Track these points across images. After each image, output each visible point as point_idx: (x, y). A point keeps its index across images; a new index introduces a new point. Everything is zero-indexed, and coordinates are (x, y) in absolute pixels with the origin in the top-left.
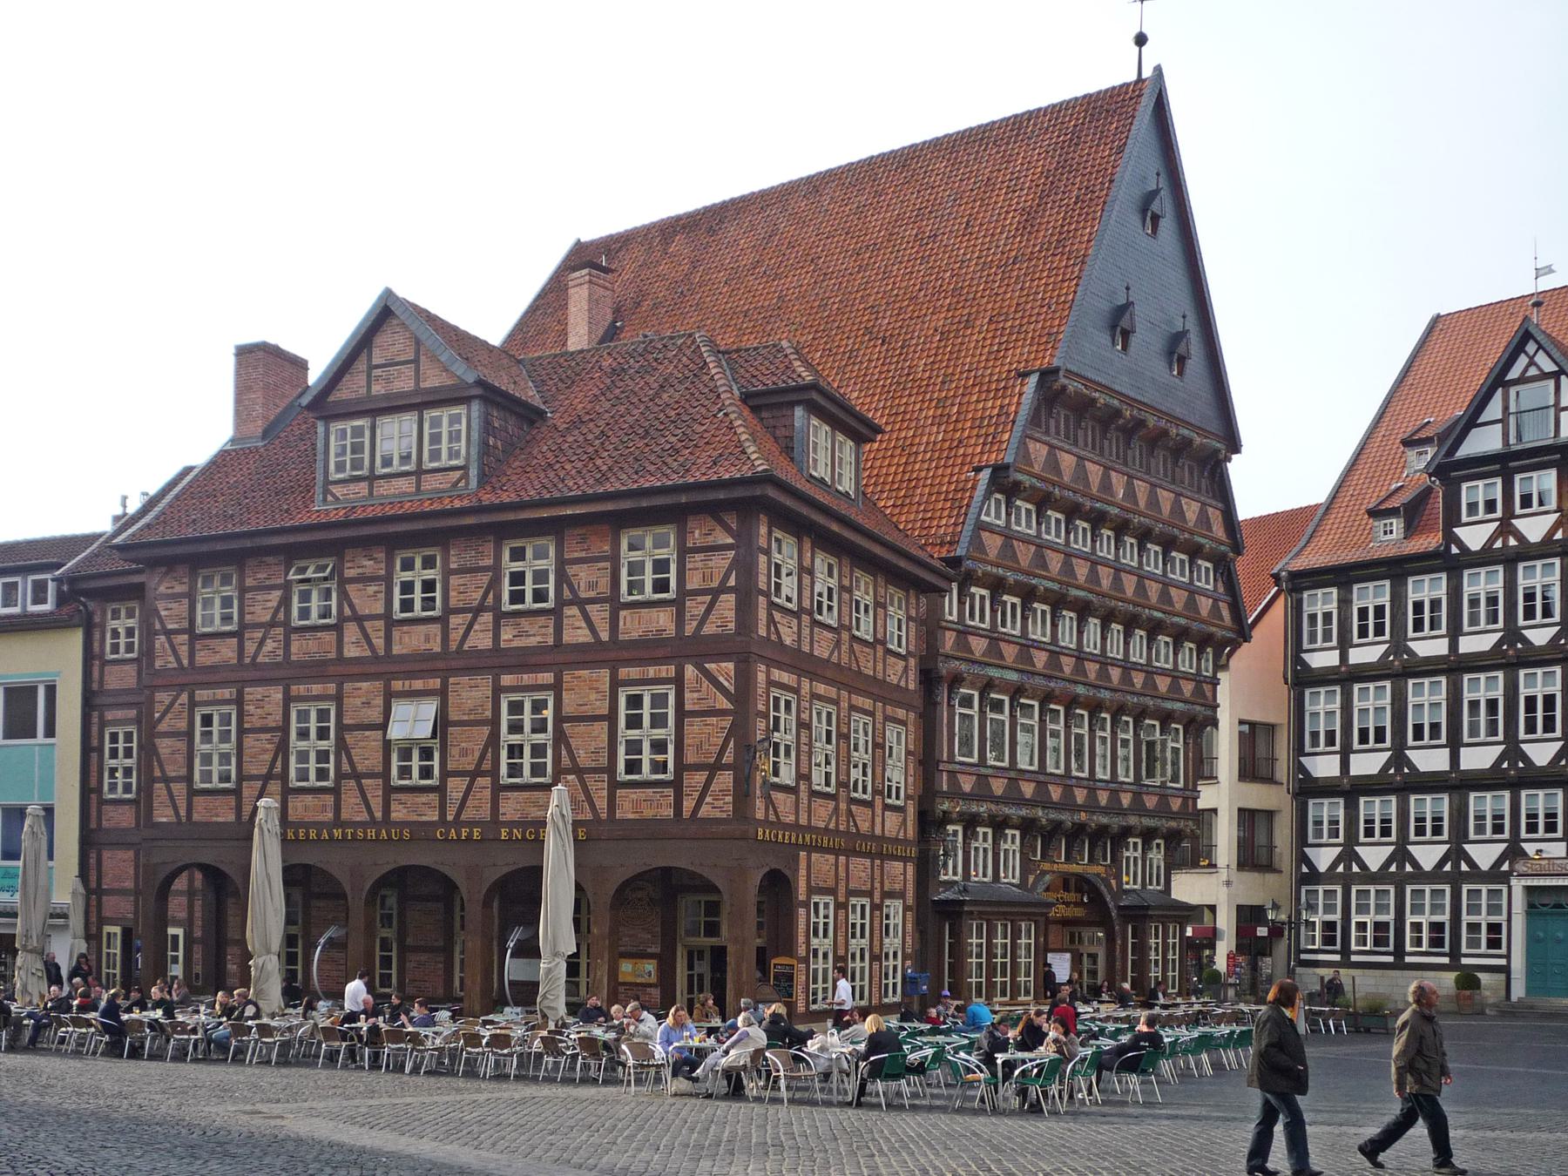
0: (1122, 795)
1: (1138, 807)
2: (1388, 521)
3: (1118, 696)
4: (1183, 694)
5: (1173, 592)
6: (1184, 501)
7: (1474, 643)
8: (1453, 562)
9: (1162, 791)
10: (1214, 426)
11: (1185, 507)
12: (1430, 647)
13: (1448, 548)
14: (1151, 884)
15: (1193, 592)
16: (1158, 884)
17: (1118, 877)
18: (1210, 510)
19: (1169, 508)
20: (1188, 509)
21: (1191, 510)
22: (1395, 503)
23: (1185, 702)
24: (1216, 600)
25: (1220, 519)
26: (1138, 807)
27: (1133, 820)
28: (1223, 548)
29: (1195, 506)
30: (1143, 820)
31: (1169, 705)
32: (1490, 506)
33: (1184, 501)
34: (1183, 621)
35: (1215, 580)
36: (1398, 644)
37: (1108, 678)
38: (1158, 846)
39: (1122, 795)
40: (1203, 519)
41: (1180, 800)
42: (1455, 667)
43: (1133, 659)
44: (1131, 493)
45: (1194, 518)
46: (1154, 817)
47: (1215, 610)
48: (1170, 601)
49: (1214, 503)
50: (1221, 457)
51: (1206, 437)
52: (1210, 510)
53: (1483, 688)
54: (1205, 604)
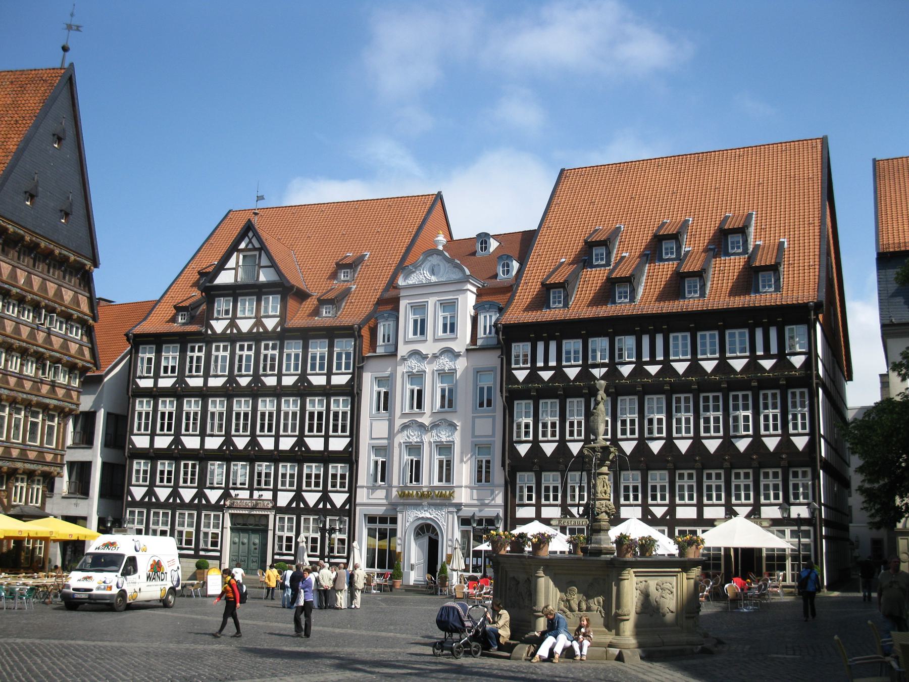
0: (13, 450)
1: (23, 458)
2: (183, 313)
3: (13, 394)
4: (57, 395)
5: (53, 338)
6: (63, 289)
7: (214, 382)
8: (210, 339)
9: (40, 449)
10: (88, 252)
11: (64, 293)
12: (196, 382)
13: (207, 331)
14: (31, 502)
15: (66, 340)
16: (37, 502)
17: (9, 497)
18: (80, 296)
19: (53, 292)
20: (66, 294)
21: (68, 295)
22: (184, 304)
23: (59, 400)
24: (81, 345)
25: (86, 301)
26: (23, 458)
27: (19, 465)
28: (86, 317)
29: (71, 293)
30: (26, 465)
31: (47, 401)
32: (227, 312)
33: (63, 289)
34: (58, 355)
35: (82, 335)
36: (181, 379)
37: (8, 383)
38: (39, 481)
39: (13, 450)
40: (76, 301)
41: (52, 456)
42: (204, 394)
43: (25, 373)
44: (29, 281)
45: (69, 299)
46: (34, 464)
47: (80, 351)
48: (51, 343)
49: (83, 293)
50: (87, 268)
51: (79, 257)
52: (80, 296)
53: (217, 406)
54: (73, 348)
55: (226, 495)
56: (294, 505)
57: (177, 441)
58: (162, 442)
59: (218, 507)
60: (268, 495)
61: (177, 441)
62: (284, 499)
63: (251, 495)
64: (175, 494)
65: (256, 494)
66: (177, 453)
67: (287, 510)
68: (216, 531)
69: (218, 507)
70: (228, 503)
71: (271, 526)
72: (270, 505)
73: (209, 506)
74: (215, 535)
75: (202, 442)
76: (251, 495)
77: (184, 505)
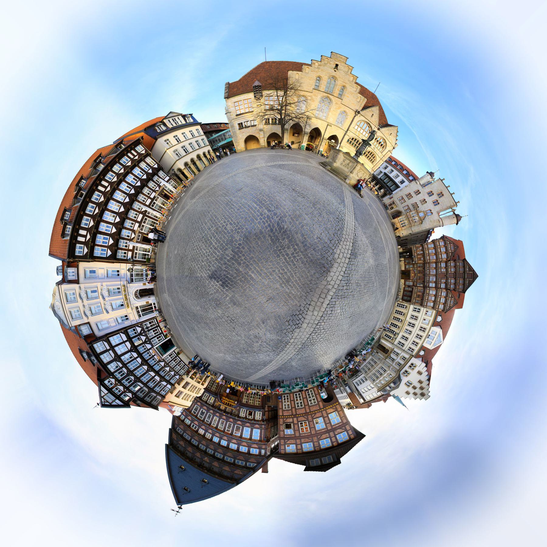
55: (160, 361)
56: (148, 342)
57: (161, 381)
58: (164, 383)
59: (164, 361)
60: (151, 351)
61: (161, 381)
62: (149, 346)
63: (154, 355)
64: (170, 371)
65: (153, 354)
66: (163, 378)
67: (150, 343)
68: (169, 357)
69: (164, 361)
70: (161, 359)
71: (158, 345)
72: (152, 349)
73: (165, 362)
74: (170, 356)
75: (155, 376)
76: (154, 355)
77: (170, 367)
